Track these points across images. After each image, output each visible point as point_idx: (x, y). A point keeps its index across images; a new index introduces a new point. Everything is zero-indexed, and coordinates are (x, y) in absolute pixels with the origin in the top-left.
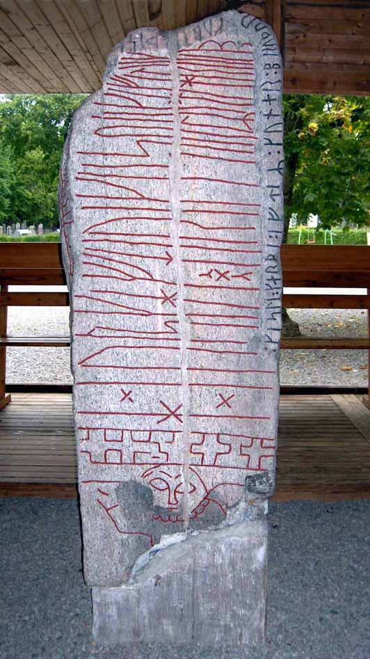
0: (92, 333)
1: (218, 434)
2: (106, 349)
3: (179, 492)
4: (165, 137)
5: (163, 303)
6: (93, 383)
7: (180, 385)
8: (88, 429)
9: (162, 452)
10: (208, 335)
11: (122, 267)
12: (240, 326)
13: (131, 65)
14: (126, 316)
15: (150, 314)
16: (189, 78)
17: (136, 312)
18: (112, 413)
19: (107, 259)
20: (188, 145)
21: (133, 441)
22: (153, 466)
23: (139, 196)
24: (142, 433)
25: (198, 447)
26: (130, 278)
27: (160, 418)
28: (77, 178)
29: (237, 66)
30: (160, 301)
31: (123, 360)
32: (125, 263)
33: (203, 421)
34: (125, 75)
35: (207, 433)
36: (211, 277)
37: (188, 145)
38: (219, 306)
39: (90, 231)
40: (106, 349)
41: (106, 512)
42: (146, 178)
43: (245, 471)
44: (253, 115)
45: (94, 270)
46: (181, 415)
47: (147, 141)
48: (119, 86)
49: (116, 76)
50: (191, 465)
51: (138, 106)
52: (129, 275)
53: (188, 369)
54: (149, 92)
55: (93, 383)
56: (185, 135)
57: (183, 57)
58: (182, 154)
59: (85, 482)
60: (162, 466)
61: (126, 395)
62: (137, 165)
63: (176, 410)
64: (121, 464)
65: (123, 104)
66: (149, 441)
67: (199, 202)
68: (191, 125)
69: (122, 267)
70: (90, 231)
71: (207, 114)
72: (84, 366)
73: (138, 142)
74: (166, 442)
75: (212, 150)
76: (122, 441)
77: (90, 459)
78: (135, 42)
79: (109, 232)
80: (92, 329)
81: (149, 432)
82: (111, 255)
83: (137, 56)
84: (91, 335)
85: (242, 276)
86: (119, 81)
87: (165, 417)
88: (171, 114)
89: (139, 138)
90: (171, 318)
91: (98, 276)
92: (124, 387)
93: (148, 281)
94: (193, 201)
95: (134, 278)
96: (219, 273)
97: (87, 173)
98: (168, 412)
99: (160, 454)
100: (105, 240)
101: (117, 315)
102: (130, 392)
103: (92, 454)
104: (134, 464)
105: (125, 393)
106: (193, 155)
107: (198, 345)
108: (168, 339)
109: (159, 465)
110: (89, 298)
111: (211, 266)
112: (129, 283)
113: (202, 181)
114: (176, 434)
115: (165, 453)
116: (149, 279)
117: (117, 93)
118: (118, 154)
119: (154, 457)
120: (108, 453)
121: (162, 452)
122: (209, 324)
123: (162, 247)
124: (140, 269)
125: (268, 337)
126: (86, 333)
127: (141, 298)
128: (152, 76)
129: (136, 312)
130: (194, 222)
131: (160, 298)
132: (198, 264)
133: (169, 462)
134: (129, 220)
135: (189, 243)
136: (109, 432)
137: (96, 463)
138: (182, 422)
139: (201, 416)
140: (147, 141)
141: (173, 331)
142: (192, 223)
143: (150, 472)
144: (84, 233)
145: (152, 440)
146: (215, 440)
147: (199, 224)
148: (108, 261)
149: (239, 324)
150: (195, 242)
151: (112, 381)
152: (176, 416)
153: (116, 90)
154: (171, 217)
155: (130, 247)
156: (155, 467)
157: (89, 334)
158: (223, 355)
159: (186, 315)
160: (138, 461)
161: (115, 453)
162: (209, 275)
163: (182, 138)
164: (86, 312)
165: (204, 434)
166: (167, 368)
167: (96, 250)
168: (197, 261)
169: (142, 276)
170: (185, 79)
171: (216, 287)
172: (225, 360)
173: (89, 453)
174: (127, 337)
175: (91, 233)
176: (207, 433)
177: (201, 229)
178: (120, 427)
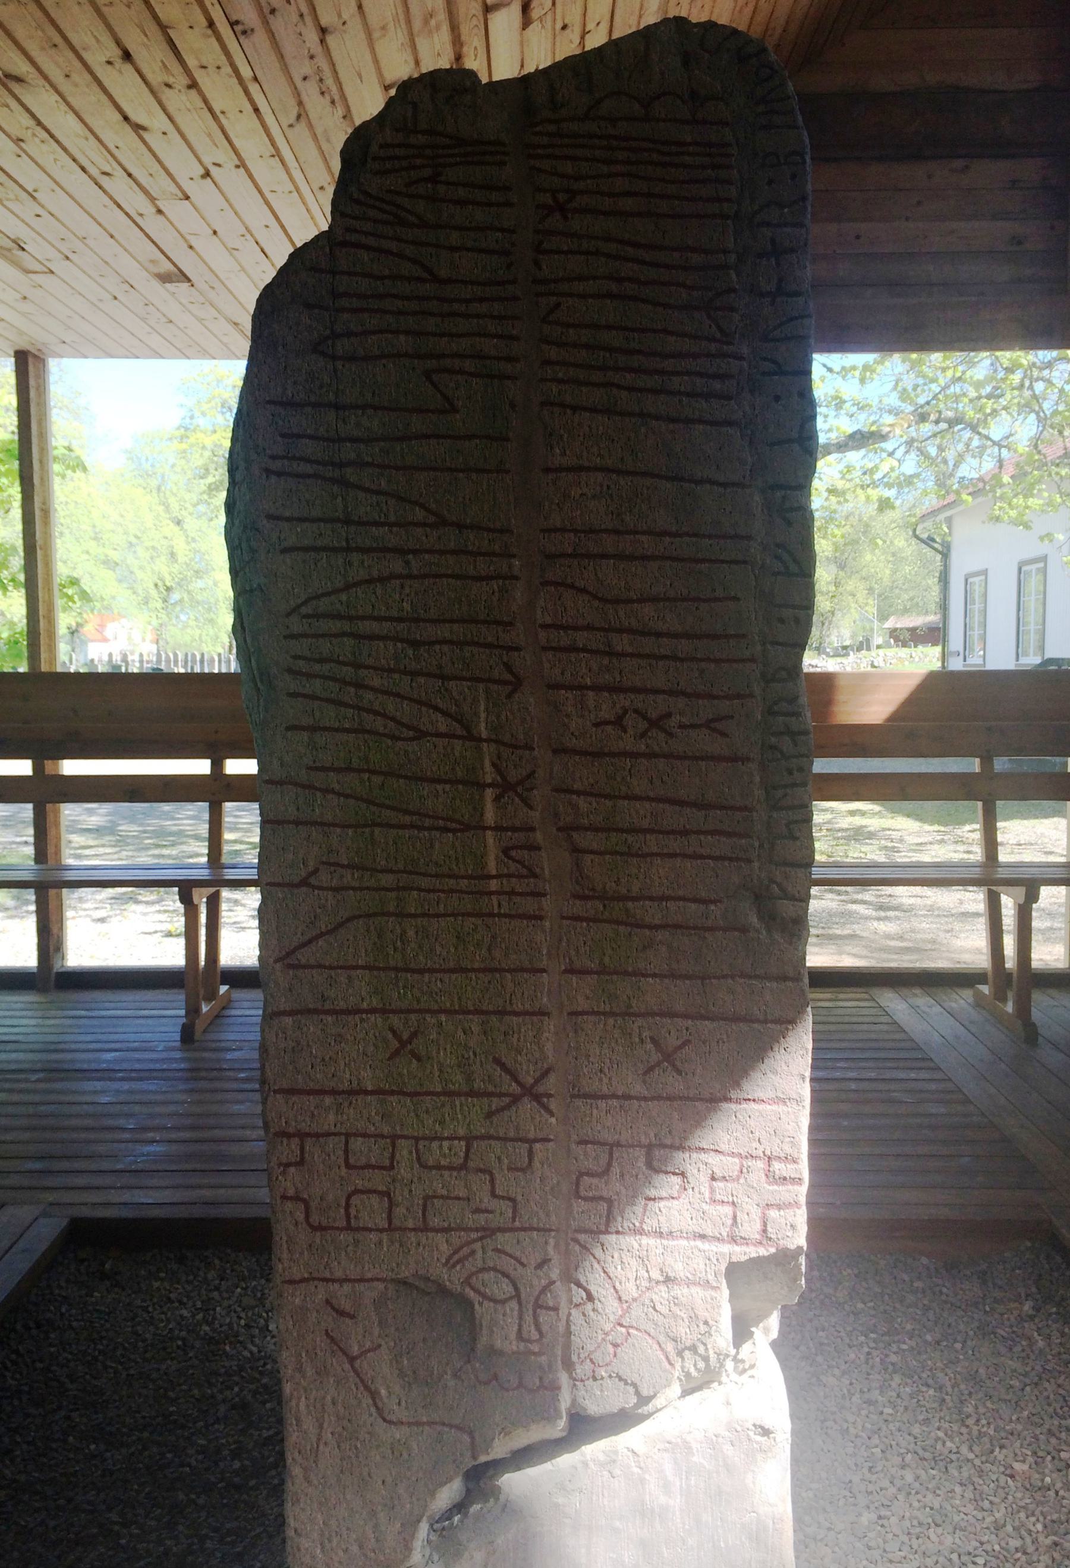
0: (313, 881)
1: (650, 1147)
2: (349, 920)
3: (548, 1308)
4: (499, 359)
5: (497, 799)
6: (316, 1011)
7: (548, 1014)
8: (302, 1136)
9: (503, 1198)
10: (618, 882)
11: (391, 705)
12: (702, 857)
13: (405, 163)
14: (401, 832)
15: (467, 828)
16: (562, 197)
17: (427, 822)
18: (366, 1092)
19: (350, 684)
20: (560, 381)
21: (421, 1165)
22: (474, 1235)
23: (432, 519)
24: (446, 1144)
25: (595, 1181)
26: (411, 733)
27: (495, 1103)
28: (268, 472)
29: (687, 159)
30: (489, 793)
31: (395, 950)
32: (398, 695)
33: (608, 1112)
34: (389, 191)
35: (618, 1144)
36: (625, 732)
37: (560, 381)
38: (647, 805)
39: (304, 610)
40: (349, 920)
41: (347, 1366)
42: (450, 469)
43: (726, 1248)
44: (733, 295)
45: (317, 714)
46: (550, 1096)
47: (450, 371)
48: (375, 221)
49: (366, 193)
50: (576, 1231)
51: (425, 275)
52: (409, 727)
53: (566, 971)
54: (455, 238)
55: (316, 1011)
56: (553, 353)
57: (545, 140)
58: (543, 404)
59: (291, 1282)
60: (499, 1235)
61: (403, 1044)
62: (427, 437)
63: (537, 1081)
64: (391, 1228)
65: (387, 272)
66: (464, 1166)
67: (592, 531)
68: (569, 326)
69: (391, 705)
70: (304, 610)
71: (610, 296)
72: (290, 966)
73: (428, 374)
74: (509, 1169)
75: (624, 394)
76: (392, 1167)
77: (307, 1217)
78: (415, 105)
79: (353, 612)
80: (311, 869)
81: (463, 1143)
82: (363, 672)
83: (422, 139)
84: (309, 885)
85: (708, 724)
86: (374, 207)
87: (507, 1100)
88: (515, 298)
89: (431, 364)
90: (520, 837)
91: (325, 729)
92: (395, 1020)
93: (458, 744)
94: (575, 531)
95: (420, 735)
96: (644, 717)
97: (294, 458)
98: (515, 1088)
99: (496, 1200)
100: (344, 634)
101: (377, 830)
102: (414, 1035)
103: (313, 1205)
104: (426, 1229)
105: (400, 1041)
106: (575, 409)
107: (593, 907)
108: (512, 893)
109: (488, 1232)
110: (304, 787)
111: (624, 701)
112: (413, 747)
113: (600, 476)
114: (537, 1146)
115: (510, 1199)
116: (459, 737)
117: (371, 241)
118: (375, 408)
119: (478, 1211)
120: (355, 1200)
121: (503, 1198)
122: (622, 854)
123: (497, 652)
124: (436, 709)
125: (779, 885)
126: (296, 880)
127: (439, 787)
128: (461, 192)
129: (427, 822)
130: (577, 584)
131: (490, 785)
132: (591, 693)
133: (517, 1224)
134: (408, 582)
135: (564, 639)
136: (357, 1144)
137: (321, 1228)
138: (552, 1114)
139: (604, 1097)
140: (450, 371)
141: (525, 872)
142: (572, 586)
143: (466, 1250)
144: (288, 615)
145: (471, 1164)
146: (641, 1163)
147: (591, 589)
148: (352, 690)
149: (703, 851)
150: (581, 638)
151: (365, 1005)
152: (537, 1098)
153: (366, 234)
154: (516, 571)
155: (410, 652)
156: (481, 1239)
157: (304, 883)
158: (660, 935)
159: (559, 829)
160: (435, 1221)
161: (374, 1200)
162: (618, 722)
163: (547, 362)
164: (297, 823)
165: (612, 1146)
166: (509, 971)
167: (321, 661)
168: (588, 688)
169: (443, 728)
170: (550, 202)
171: (634, 755)
172: (664, 949)
173: (304, 1201)
174: (404, 889)
175: (307, 616)
176: (618, 1144)
177: (596, 603)
178: (386, 1130)
